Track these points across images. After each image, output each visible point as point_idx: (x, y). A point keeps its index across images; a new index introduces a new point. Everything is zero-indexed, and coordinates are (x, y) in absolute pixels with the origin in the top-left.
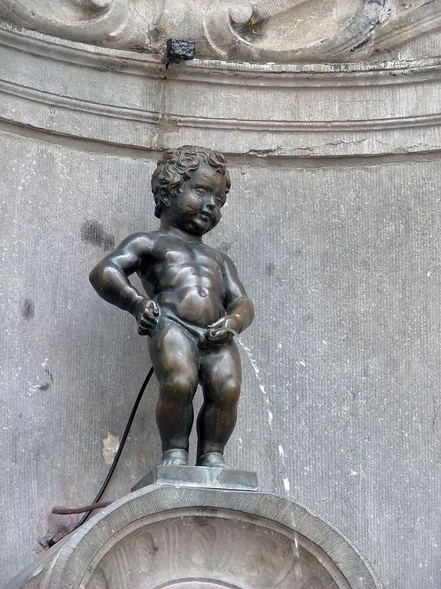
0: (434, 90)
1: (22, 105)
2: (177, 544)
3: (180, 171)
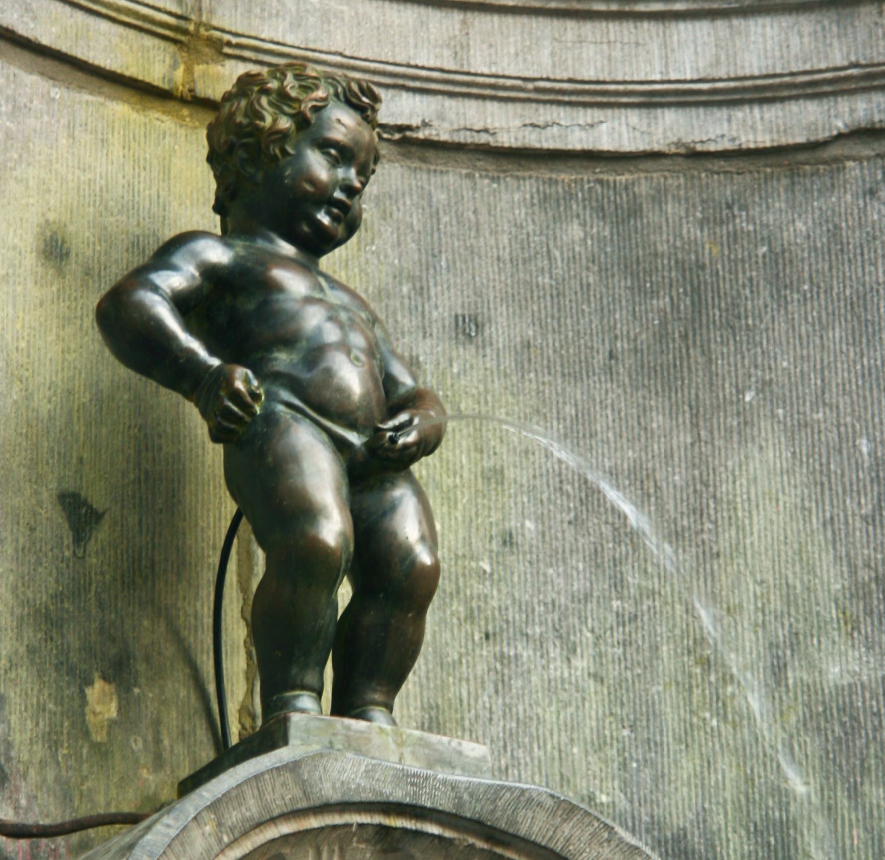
0: (752, 29)
3: (286, 108)
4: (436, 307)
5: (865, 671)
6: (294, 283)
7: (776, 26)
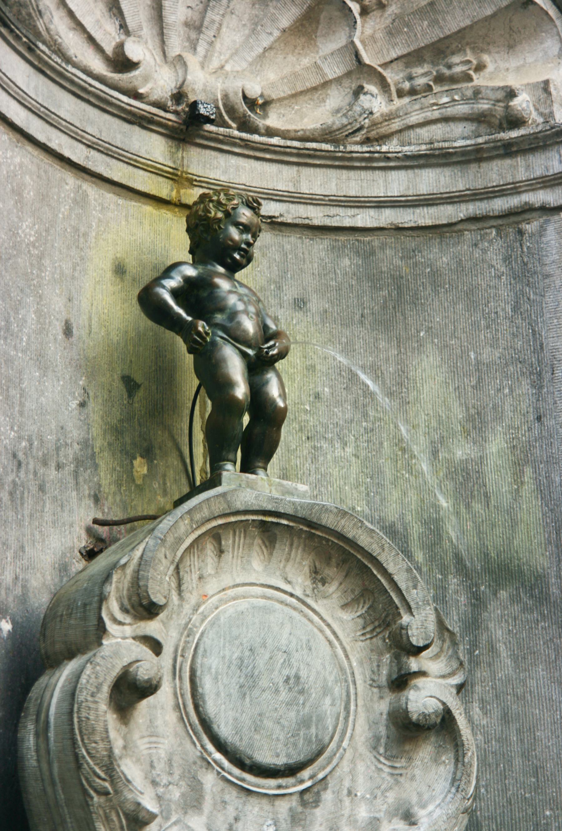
1: (64, 138)
2: (241, 549)
3: (221, 208)
4: (286, 295)
5: (473, 453)
6: (224, 285)
7: (434, 172)
